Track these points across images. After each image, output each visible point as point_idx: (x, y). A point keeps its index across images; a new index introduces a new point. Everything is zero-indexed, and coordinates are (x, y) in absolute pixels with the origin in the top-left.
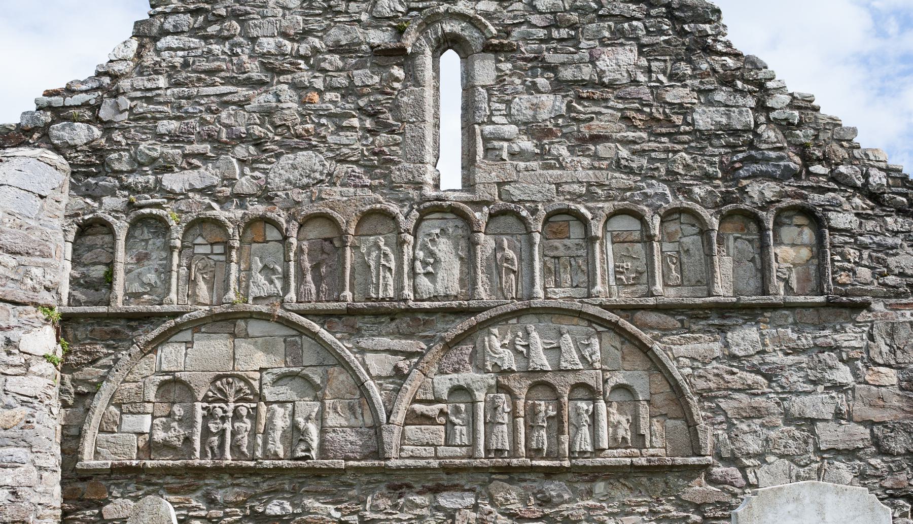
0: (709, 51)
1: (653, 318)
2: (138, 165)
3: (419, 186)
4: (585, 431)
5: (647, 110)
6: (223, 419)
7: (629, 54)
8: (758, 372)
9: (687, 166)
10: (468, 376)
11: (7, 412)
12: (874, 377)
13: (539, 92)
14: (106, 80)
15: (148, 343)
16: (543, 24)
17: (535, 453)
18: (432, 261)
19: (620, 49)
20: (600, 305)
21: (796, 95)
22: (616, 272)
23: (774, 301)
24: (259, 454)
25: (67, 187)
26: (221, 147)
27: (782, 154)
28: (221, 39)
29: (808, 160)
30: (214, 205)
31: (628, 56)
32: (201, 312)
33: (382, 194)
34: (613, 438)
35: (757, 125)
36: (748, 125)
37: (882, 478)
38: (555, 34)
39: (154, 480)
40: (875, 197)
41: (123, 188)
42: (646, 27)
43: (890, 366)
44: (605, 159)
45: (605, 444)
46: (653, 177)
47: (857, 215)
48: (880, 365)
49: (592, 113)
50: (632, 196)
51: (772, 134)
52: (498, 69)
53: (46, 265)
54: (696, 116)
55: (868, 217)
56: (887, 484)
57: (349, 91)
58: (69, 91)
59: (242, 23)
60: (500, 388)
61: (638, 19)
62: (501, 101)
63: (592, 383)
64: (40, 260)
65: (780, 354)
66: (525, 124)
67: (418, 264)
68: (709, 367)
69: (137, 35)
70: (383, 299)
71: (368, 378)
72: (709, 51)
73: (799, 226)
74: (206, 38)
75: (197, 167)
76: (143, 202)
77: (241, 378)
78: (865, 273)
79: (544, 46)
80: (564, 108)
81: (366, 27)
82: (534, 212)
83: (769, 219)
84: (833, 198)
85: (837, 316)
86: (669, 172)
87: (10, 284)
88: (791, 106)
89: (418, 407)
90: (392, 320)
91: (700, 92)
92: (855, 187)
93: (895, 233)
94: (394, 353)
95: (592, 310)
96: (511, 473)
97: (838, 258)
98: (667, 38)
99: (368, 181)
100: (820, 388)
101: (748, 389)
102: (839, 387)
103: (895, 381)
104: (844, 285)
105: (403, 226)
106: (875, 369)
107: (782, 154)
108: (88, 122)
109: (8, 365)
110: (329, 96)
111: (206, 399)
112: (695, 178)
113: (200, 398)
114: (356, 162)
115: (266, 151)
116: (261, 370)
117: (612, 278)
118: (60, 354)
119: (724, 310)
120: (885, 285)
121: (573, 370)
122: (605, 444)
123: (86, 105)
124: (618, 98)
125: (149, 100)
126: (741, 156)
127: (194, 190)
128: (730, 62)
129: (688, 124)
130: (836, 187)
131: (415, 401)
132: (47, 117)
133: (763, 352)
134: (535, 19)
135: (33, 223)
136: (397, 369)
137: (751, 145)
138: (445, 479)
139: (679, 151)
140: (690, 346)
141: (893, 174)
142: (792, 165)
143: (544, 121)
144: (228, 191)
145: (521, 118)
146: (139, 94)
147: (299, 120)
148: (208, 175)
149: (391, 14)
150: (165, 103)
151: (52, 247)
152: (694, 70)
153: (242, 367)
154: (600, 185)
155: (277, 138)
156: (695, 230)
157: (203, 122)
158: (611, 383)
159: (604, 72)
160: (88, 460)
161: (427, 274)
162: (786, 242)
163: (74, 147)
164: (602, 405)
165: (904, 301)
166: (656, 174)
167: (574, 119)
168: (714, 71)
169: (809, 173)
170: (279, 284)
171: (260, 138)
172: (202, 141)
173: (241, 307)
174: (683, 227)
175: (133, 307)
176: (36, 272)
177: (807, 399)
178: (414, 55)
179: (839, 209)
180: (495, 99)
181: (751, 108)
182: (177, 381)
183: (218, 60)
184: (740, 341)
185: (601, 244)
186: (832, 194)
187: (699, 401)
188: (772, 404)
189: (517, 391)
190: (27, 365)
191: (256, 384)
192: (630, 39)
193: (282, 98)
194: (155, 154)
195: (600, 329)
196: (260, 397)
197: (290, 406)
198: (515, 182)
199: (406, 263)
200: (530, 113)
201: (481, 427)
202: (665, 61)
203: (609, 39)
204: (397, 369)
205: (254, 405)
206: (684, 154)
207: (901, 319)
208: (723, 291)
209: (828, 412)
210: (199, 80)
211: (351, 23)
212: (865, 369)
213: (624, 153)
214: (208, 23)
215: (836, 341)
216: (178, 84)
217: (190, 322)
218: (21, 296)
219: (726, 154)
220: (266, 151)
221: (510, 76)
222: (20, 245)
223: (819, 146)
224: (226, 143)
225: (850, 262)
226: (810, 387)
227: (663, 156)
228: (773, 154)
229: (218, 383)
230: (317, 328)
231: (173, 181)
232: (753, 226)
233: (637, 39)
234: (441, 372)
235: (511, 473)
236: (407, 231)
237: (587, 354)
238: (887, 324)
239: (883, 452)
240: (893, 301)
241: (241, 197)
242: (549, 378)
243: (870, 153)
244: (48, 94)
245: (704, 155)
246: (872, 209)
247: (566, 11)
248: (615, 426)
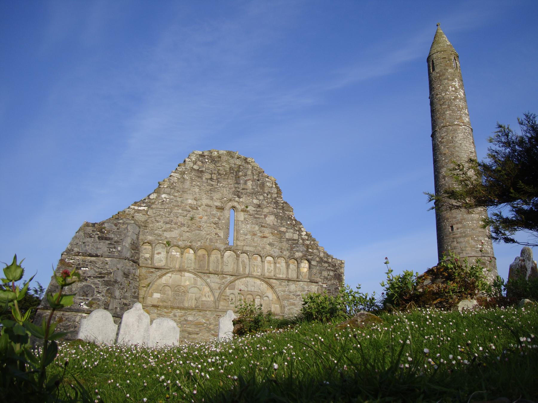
1: (274, 281)
39: (162, 310)
63: (261, 295)
77: (183, 286)
85: (311, 285)
90: (218, 276)
119: (289, 280)
156: (284, 262)
195: (263, 283)
229: (177, 287)
232: (296, 262)
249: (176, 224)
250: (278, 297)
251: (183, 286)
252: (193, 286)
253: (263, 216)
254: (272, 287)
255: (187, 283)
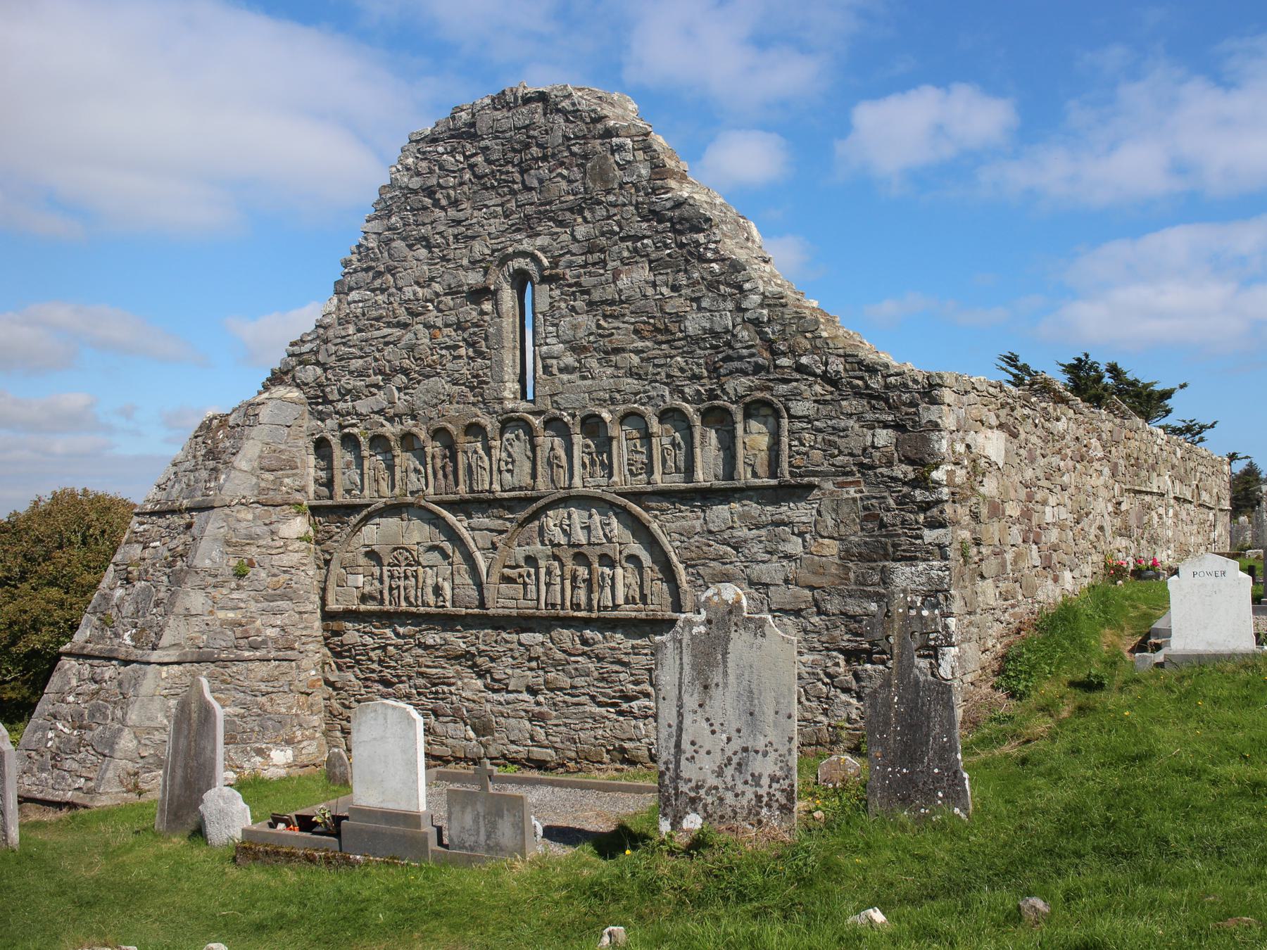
0: (702, 259)
2: (343, 394)
3: (501, 400)
4: (608, 590)
5: (652, 321)
6: (399, 578)
7: (641, 271)
8: (729, 545)
9: (682, 370)
10: (537, 548)
11: (275, 579)
12: (818, 549)
13: (577, 313)
14: (321, 331)
15: (355, 526)
16: (581, 252)
17: (576, 607)
18: (510, 460)
19: (634, 267)
20: (615, 492)
21: (767, 294)
22: (629, 464)
23: (738, 485)
24: (420, 603)
25: (307, 415)
26: (388, 378)
27: (753, 350)
28: (383, 291)
29: (775, 353)
30: (385, 422)
31: (643, 273)
32: (380, 503)
33: (480, 408)
34: (627, 598)
35: (734, 326)
36: (726, 328)
37: (819, 633)
38: (590, 259)
40: (831, 380)
41: (337, 413)
42: (654, 244)
43: (833, 538)
44: (622, 368)
45: (620, 600)
46: (656, 381)
47: (815, 401)
48: (824, 537)
49: (614, 328)
50: (641, 398)
51: (745, 333)
52: (551, 297)
53: (294, 475)
54: (688, 323)
55: (826, 402)
56: (823, 639)
57: (459, 326)
58: (303, 341)
59: (393, 275)
60: (556, 557)
61: (648, 237)
62: (553, 325)
63: (611, 554)
64: (290, 472)
65: (745, 530)
66: (568, 342)
67: (503, 463)
68: (692, 540)
69: (337, 293)
70: (482, 492)
71: (475, 549)
72: (702, 259)
73: (765, 416)
74: (373, 291)
75: (375, 394)
76: (347, 423)
77: (407, 550)
78: (817, 455)
79: (582, 271)
80: (594, 326)
81: (466, 269)
82: (573, 416)
83: (737, 411)
84: (795, 388)
86: (668, 376)
87: (271, 493)
88: (762, 306)
89: (506, 571)
91: (692, 300)
92: (815, 375)
93: (850, 415)
94: (491, 531)
95: (609, 497)
96: (567, 622)
97: (796, 443)
98: (669, 251)
99: (472, 399)
100: (775, 558)
101: (720, 558)
102: (788, 557)
103: (835, 551)
104: (799, 467)
105: (490, 435)
106: (820, 540)
107: (753, 350)
108: (313, 364)
109: (271, 547)
110: (446, 331)
111: (389, 565)
112: (690, 379)
113: (386, 563)
114: (463, 384)
115: (412, 379)
116: (418, 543)
117: (626, 468)
118: (312, 533)
120: (833, 465)
121: (598, 544)
122: (620, 600)
123: (312, 351)
124: (632, 313)
125: (344, 344)
126: (720, 356)
127: (373, 412)
128: (715, 266)
129: (681, 331)
130: (798, 377)
131: (505, 567)
132: (293, 361)
133: (732, 528)
134: (575, 248)
135: (282, 447)
136: (493, 543)
137: (728, 344)
138: (524, 624)
139: (674, 356)
140: (678, 524)
141: (850, 359)
142: (760, 361)
143: (581, 338)
144: (392, 412)
145: (565, 338)
146: (339, 340)
147: (429, 352)
148: (381, 398)
149: (481, 257)
150: (354, 346)
151: (298, 460)
152: (688, 279)
153: (406, 542)
154: (619, 391)
155: (417, 368)
157: (376, 360)
158: (625, 554)
159: (621, 290)
160: (333, 606)
161: (508, 471)
162: (753, 431)
163: (307, 384)
164: (619, 571)
165: (850, 479)
166: (658, 378)
167: (600, 335)
168: (703, 278)
169: (776, 367)
170: (423, 481)
171: (407, 369)
172: (375, 374)
173: (401, 500)
174: (676, 423)
175: (348, 500)
176: (286, 481)
177: (763, 566)
178: (496, 291)
179: (799, 398)
180: (548, 323)
181: (730, 311)
182: (373, 552)
183: (381, 308)
184: (716, 519)
185: (618, 442)
186: (795, 384)
187: (686, 568)
188: (737, 570)
189: (564, 560)
190: (285, 545)
191: (415, 554)
192: (642, 256)
193: (419, 337)
194: (349, 387)
196: (419, 564)
197: (435, 569)
198: (561, 393)
199: (494, 462)
200: (570, 333)
201: (543, 588)
202: (667, 274)
203: (628, 258)
204: (493, 543)
205: (415, 568)
206: (679, 359)
207: (846, 496)
208: (704, 475)
209: (779, 579)
210: (372, 326)
211: (456, 268)
212: (812, 541)
213: (635, 359)
214: (374, 278)
215: (789, 517)
216: (360, 331)
217: (376, 511)
218: (279, 499)
219: (710, 355)
220: (412, 379)
221: (559, 301)
222: (275, 464)
223: (785, 340)
224: (389, 375)
225: (804, 446)
226: (767, 557)
227: (662, 361)
228: (745, 352)
230: (445, 513)
231: (363, 406)
233: (648, 255)
234: (519, 546)
235: (567, 622)
236: (493, 439)
237: (607, 531)
238: (833, 501)
239: (820, 612)
240: (840, 479)
241: (400, 416)
242: (584, 550)
243: (829, 341)
244: (292, 344)
245: (693, 358)
246: (832, 393)
247: (597, 237)
248: (627, 586)
251: (407, 550)
252: (430, 543)
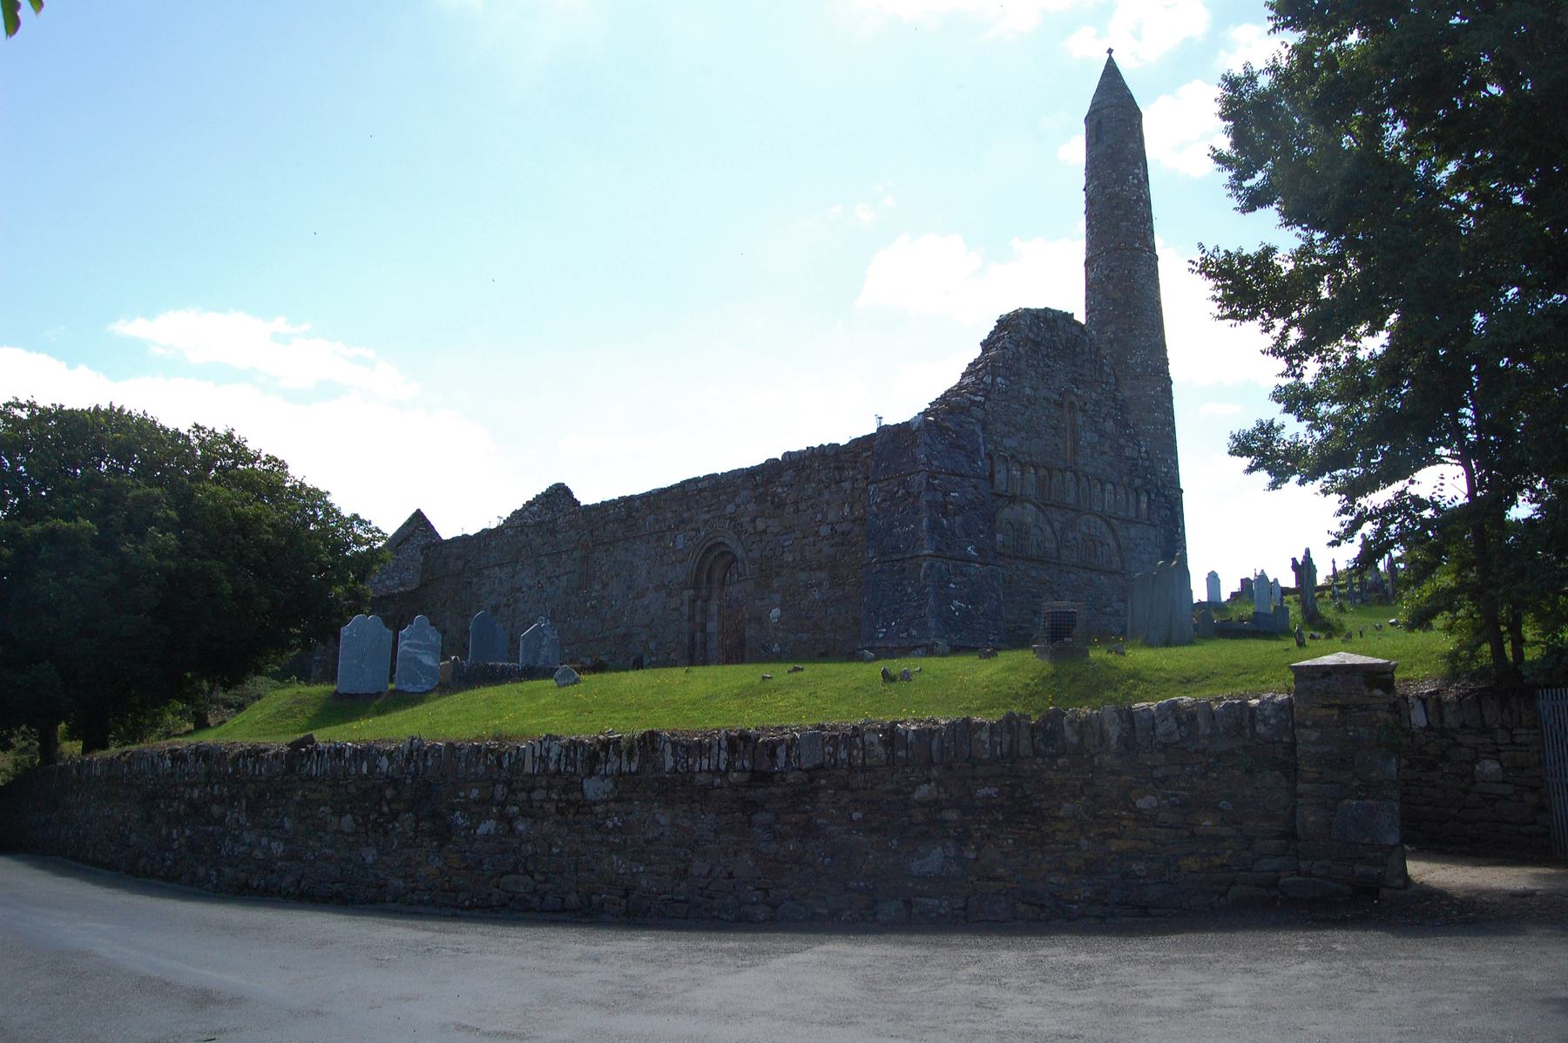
1: (1115, 521)
249: (1014, 426)
250: (1119, 546)
253: (1101, 420)
254: (1113, 531)
255: (1030, 520)
